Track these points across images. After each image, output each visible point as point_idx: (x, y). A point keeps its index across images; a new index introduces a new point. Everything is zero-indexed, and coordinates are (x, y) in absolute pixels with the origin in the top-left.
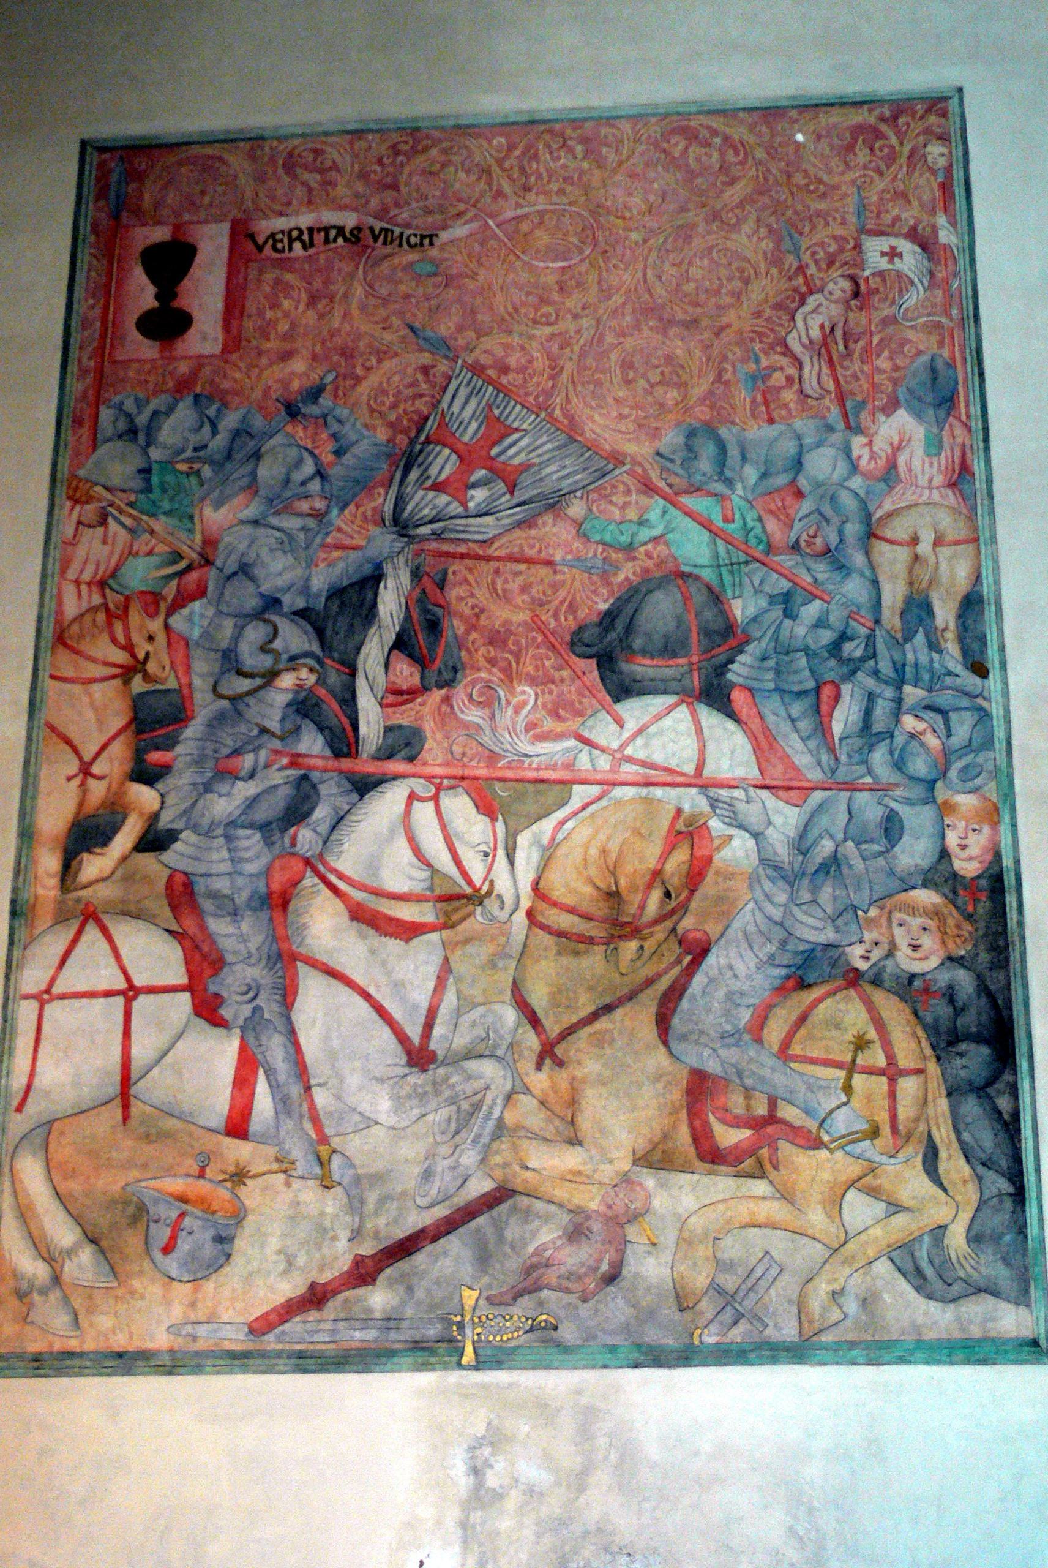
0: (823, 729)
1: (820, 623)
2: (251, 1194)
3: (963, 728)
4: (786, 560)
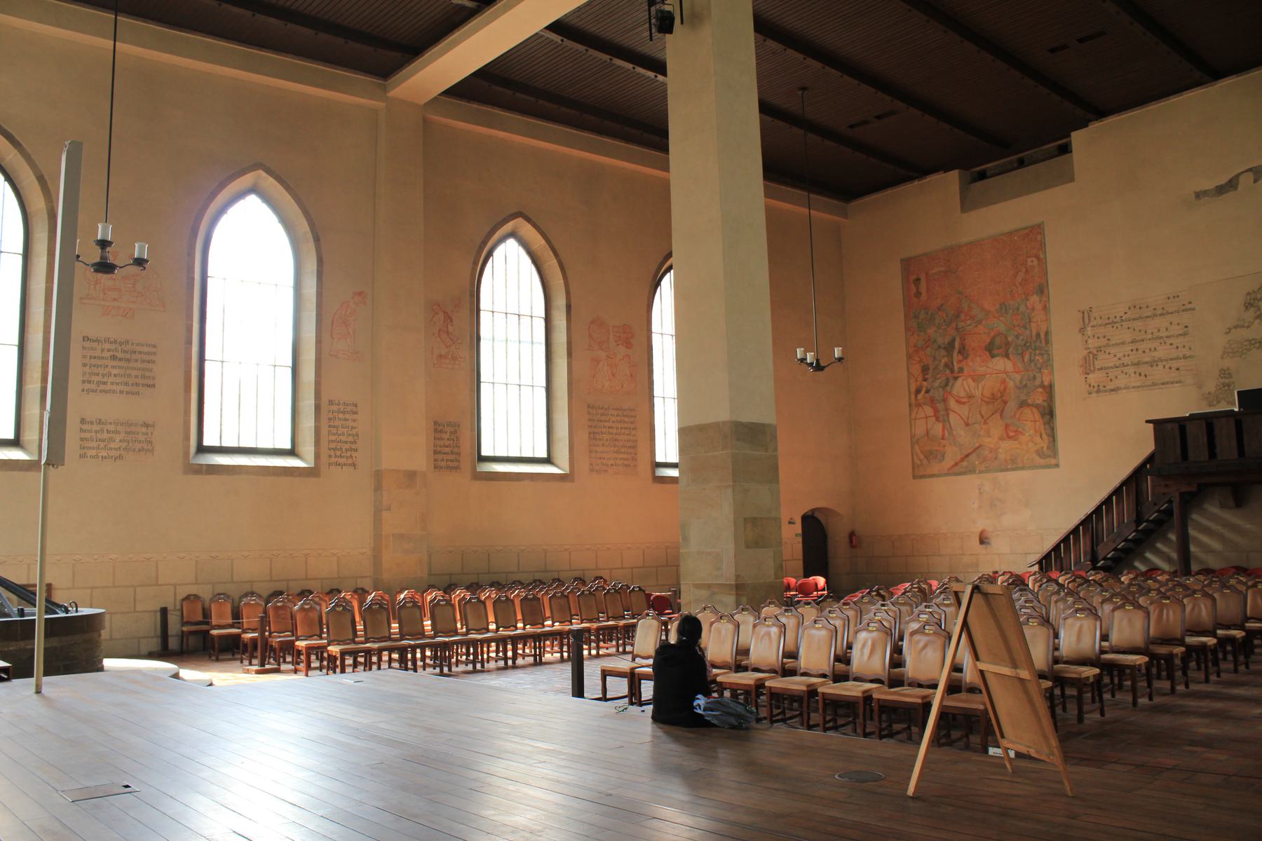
0: (1023, 360)
1: (1023, 340)
2: (946, 448)
4: (1017, 328)
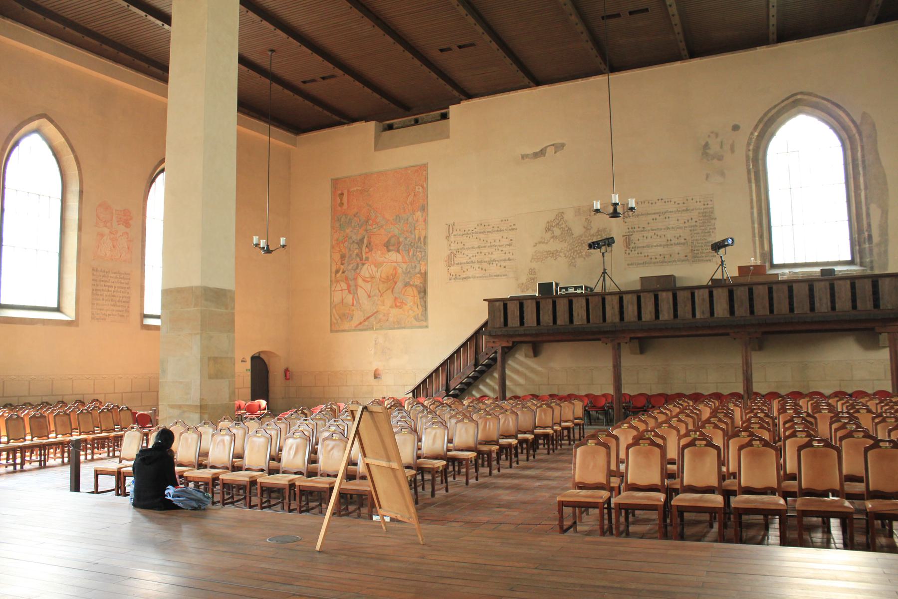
0: (409, 255)
1: (409, 241)
2: (354, 312)
3: (423, 253)
